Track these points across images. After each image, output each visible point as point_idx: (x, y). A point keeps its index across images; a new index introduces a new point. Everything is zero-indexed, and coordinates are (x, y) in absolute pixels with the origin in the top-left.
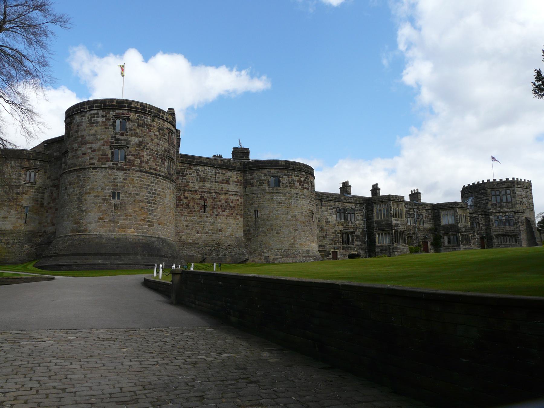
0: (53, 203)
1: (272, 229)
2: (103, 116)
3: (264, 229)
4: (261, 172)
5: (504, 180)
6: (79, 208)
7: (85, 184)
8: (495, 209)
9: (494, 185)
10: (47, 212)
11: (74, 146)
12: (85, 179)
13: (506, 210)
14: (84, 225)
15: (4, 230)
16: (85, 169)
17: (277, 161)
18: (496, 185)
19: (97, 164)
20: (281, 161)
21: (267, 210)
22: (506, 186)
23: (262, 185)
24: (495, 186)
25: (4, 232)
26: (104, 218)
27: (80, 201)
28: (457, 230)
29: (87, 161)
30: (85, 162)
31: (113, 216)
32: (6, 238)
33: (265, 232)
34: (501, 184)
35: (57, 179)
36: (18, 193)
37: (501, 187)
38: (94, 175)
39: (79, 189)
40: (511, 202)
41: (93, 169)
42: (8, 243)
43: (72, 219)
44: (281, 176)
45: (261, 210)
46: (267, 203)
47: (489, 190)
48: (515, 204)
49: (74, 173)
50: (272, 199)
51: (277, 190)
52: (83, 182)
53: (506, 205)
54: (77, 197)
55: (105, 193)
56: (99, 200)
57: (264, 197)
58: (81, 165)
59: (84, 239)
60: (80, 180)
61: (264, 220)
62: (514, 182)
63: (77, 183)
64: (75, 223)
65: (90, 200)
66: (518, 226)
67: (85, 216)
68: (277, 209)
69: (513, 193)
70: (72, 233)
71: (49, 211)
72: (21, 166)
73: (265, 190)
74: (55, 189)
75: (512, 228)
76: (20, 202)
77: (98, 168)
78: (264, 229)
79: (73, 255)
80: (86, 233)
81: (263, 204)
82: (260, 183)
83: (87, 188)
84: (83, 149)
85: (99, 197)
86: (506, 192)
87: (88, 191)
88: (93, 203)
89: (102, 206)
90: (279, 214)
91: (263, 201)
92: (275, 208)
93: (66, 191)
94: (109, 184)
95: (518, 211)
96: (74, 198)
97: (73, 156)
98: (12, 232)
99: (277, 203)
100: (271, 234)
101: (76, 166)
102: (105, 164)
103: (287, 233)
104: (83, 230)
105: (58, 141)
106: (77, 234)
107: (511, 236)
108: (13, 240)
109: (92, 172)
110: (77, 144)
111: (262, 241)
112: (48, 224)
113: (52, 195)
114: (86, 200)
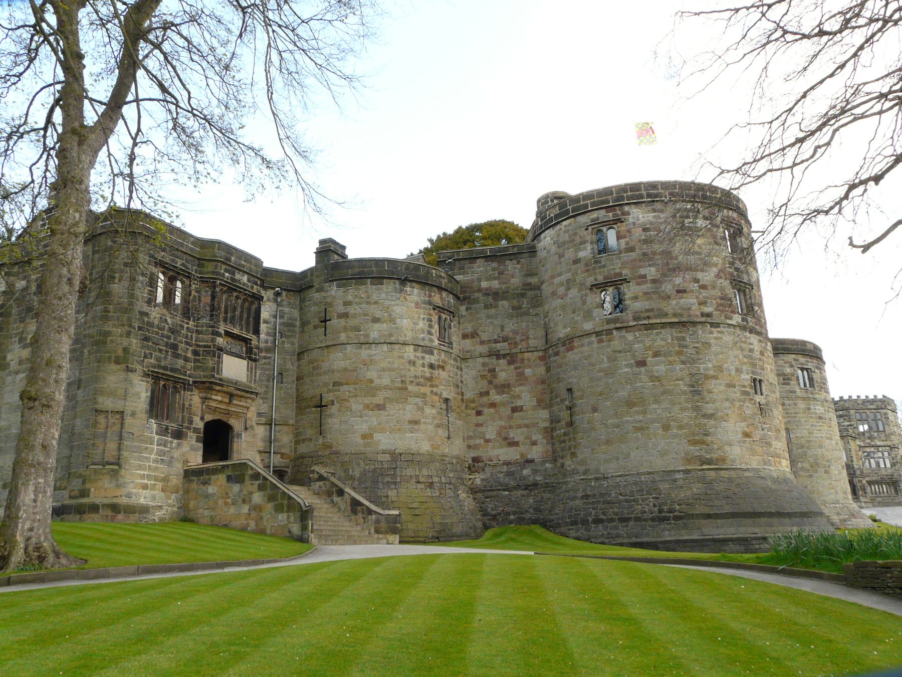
0: (498, 393)
1: (818, 464)
2: (705, 218)
3: (806, 465)
4: (783, 360)
5: (871, 397)
6: (697, 409)
7: (701, 356)
8: (864, 441)
9: (858, 404)
10: (479, 413)
11: (642, 271)
12: (697, 345)
13: (879, 443)
14: (716, 446)
15: (416, 452)
16: (694, 324)
17: (804, 343)
18: (862, 404)
19: (717, 317)
20: (809, 342)
21: (805, 429)
22: (874, 407)
23: (789, 384)
24: (861, 406)
25: (418, 458)
26: (751, 433)
27: (696, 393)
28: (852, 472)
29: (694, 308)
30: (689, 309)
31: (763, 429)
32: (425, 472)
33: (808, 471)
34: (868, 404)
35: (504, 341)
36: (431, 366)
37: (869, 407)
38: (715, 338)
39: (689, 368)
40: (884, 431)
41: (712, 325)
42: (431, 485)
43: (680, 432)
44: (813, 369)
45: (794, 429)
46: (803, 417)
47: (852, 412)
48: (889, 435)
49: (663, 331)
50: (809, 409)
51: (812, 393)
52: (694, 352)
53: (878, 435)
54: (685, 385)
55: (744, 379)
56: (736, 393)
57: (795, 404)
58: (681, 315)
59: (730, 480)
60: (686, 347)
61: (802, 447)
62: (884, 401)
63: (680, 353)
64: (695, 443)
65: (720, 392)
66: (897, 468)
67: (716, 428)
68: (818, 428)
69: (885, 418)
70: (689, 464)
71: (486, 411)
72: (430, 303)
73: (795, 392)
74: (503, 362)
75: (890, 472)
76: (437, 386)
77: (721, 325)
78: (805, 465)
79: (733, 515)
80: (725, 467)
81: (795, 417)
82: (784, 379)
83: (707, 366)
84: (678, 281)
85: (735, 387)
86: (875, 416)
87: (711, 372)
88: (727, 400)
89: (743, 406)
90: (821, 437)
91: (795, 413)
92: (815, 426)
93: (643, 369)
94: (746, 360)
95: (894, 445)
96: (677, 385)
97: (646, 294)
98: (431, 459)
99: (816, 418)
100: (819, 473)
101: (666, 315)
102: (731, 318)
103: (836, 472)
104: (717, 459)
105: (489, 256)
106: (704, 467)
107: (888, 483)
108: (438, 477)
109: (711, 333)
110: (653, 269)
111: (806, 487)
112: (487, 441)
113: (495, 377)
114: (710, 392)
